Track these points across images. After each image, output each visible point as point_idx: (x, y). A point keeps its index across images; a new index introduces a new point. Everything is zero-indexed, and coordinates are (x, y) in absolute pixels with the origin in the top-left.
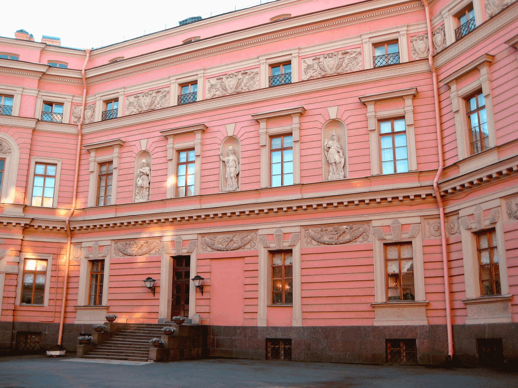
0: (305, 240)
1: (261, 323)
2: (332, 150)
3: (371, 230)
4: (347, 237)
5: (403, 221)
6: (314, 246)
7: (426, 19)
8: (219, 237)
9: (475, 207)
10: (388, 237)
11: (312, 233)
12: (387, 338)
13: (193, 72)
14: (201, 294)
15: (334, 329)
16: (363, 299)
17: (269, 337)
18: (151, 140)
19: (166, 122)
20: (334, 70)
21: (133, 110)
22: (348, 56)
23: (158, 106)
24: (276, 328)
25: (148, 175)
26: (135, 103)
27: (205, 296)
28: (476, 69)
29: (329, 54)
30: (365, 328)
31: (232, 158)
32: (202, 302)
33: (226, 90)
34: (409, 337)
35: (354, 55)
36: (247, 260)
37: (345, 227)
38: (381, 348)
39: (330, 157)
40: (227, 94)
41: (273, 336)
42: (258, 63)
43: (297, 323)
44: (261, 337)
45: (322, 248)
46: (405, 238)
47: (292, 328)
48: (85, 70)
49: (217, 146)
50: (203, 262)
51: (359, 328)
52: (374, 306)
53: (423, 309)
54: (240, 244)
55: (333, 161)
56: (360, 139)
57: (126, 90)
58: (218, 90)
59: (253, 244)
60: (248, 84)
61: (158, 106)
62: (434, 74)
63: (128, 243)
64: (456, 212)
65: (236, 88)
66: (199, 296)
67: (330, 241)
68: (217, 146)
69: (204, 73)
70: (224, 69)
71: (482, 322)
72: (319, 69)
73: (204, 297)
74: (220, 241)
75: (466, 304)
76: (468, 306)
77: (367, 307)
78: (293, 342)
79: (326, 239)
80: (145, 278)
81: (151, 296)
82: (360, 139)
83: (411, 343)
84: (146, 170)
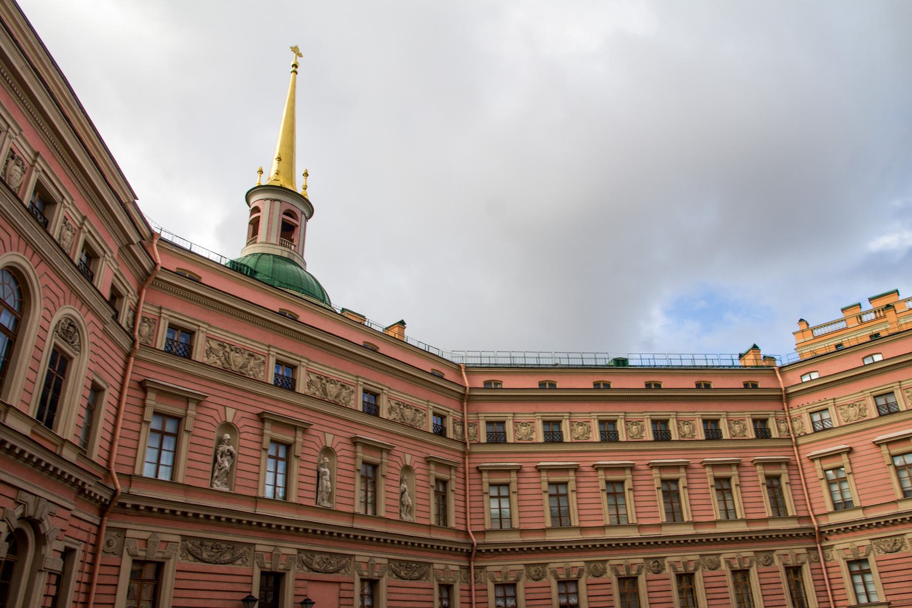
8: (317, 558)
13: (297, 356)
18: (240, 414)
19: (260, 399)
23: (251, 373)
28: (509, 471)
33: (326, 394)
36: (344, 586)
45: (400, 582)
50: (301, 583)
54: (336, 567)
58: (318, 390)
61: (251, 373)
65: (336, 397)
70: (326, 371)
79: (402, 574)
84: (231, 448)
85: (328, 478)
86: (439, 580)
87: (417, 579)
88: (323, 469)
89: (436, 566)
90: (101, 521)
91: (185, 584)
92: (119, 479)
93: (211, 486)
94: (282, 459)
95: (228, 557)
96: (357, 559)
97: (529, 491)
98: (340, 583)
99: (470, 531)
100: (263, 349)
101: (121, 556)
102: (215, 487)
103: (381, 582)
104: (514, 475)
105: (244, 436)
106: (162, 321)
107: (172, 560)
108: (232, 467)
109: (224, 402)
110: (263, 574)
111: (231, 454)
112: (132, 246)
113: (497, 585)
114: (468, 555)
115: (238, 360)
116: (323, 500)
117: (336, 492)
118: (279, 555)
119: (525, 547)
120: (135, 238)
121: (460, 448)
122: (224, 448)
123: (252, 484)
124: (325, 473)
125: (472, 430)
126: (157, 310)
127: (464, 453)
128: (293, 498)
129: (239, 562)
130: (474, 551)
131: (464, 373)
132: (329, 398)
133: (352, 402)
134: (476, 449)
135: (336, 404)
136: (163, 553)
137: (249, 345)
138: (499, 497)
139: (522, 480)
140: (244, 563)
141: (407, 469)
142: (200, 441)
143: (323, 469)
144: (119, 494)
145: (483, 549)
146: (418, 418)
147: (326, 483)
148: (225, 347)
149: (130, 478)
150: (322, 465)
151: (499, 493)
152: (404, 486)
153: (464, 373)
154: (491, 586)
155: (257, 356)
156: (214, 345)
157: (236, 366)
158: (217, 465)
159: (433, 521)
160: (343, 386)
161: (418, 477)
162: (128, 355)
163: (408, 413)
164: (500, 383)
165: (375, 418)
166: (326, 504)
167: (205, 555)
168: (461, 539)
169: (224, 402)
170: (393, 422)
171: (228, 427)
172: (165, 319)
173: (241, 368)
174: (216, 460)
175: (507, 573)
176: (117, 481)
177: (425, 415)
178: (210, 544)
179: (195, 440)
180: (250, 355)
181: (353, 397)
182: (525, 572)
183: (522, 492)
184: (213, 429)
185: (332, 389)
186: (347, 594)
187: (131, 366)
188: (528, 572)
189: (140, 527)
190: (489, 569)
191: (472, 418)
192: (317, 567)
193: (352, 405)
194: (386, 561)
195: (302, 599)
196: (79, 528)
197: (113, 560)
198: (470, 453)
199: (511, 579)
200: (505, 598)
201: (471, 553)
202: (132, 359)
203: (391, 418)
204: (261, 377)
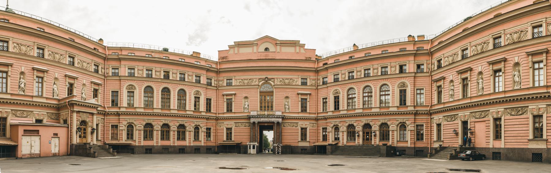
4: (520, 113)
15: (515, 149)
16: (526, 138)
22: (523, 33)
34: (540, 152)
38: (530, 156)
41: (494, 151)
43: (503, 146)
44: (491, 151)
51: (523, 148)
52: (529, 140)
53: (545, 142)
56: (526, 71)
77: (527, 141)
79: (513, 113)
82: (526, 71)
87: (521, 114)
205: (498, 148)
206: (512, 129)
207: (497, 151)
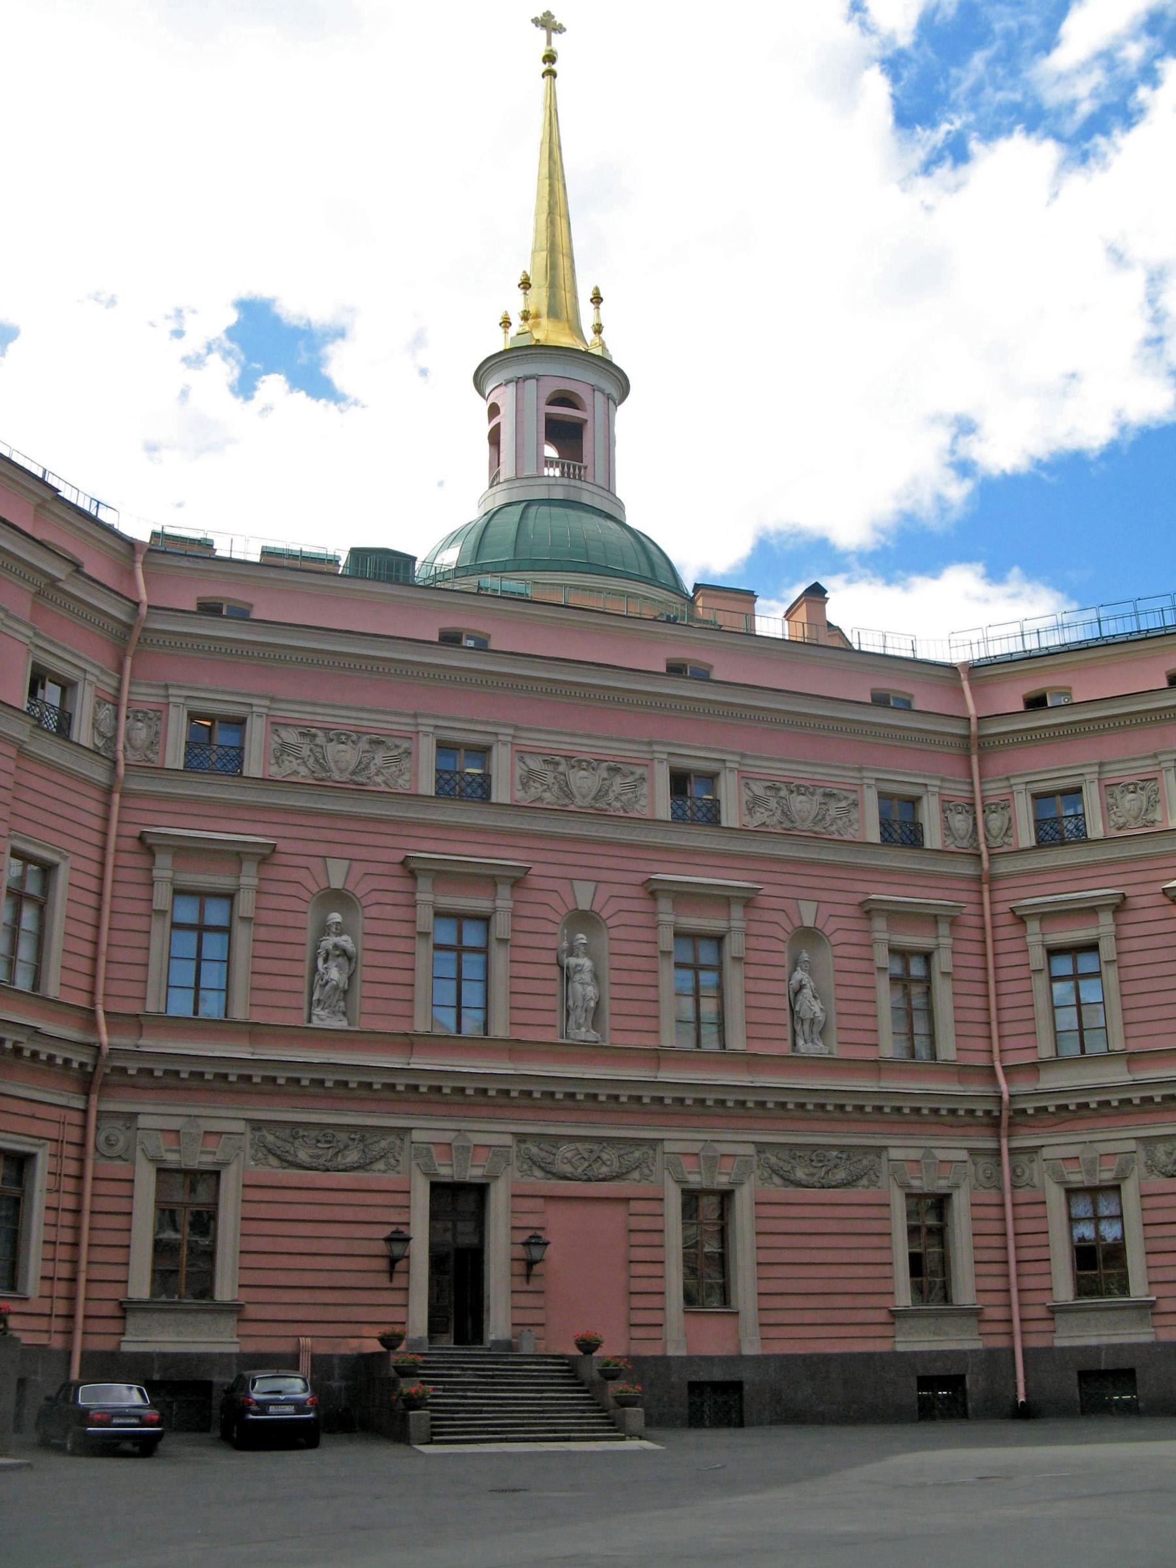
0: (758, 1172)
1: (675, 1350)
2: (807, 992)
3: (885, 1167)
4: (841, 1175)
5: (942, 1155)
6: (777, 1190)
7: (971, 776)
8: (566, 1150)
9: (1082, 1146)
10: (916, 1183)
11: (773, 1160)
12: (921, 1373)
13: (487, 723)
14: (523, 1279)
15: (827, 1359)
17: (694, 1378)
18: (359, 868)
20: (807, 825)
21: (295, 767)
22: (833, 805)
24: (709, 1360)
25: (350, 959)
26: (305, 752)
27: (535, 1284)
28: (1094, 910)
29: (801, 786)
30: (881, 1355)
31: (586, 962)
32: (524, 1300)
35: (843, 804)
36: (635, 1206)
37: (835, 1153)
38: (910, 1394)
39: (805, 1007)
40: (572, 808)
41: (703, 1376)
42: (648, 756)
43: (752, 1348)
46: (941, 1187)
47: (741, 1358)
48: (149, 607)
49: (550, 928)
51: (870, 1356)
52: (893, 1314)
53: (973, 1321)
54: (616, 1167)
55: (809, 1016)
56: (859, 980)
57: (275, 706)
59: (646, 1171)
60: (623, 798)
61: (379, 779)
62: (986, 887)
63: (301, 1133)
64: (1036, 1149)
66: (520, 1284)
67: (812, 1180)
68: (550, 928)
69: (514, 737)
70: (566, 744)
71: (1093, 1341)
72: (779, 812)
73: (530, 1288)
74: (569, 1155)
75: (1053, 1312)
76: (1057, 1316)
77: (883, 1316)
78: (746, 1387)
79: (800, 1174)
80: (387, 1231)
81: (382, 1280)
83: (956, 1382)
84: (345, 941)
85: (587, 977)
86: (903, 1186)
88: (573, 961)
89: (894, 1154)
90: (87, 1102)
91: (264, 1211)
92: (107, 1023)
93: (310, 1021)
94: (473, 950)
95: (353, 1157)
96: (669, 1147)
97: (1148, 957)
98: (628, 1200)
99: (998, 1065)
100: (402, 724)
101: (134, 1163)
102: (316, 1022)
103: (737, 1195)
104: (1106, 918)
105: (374, 911)
106: (173, 712)
107: (233, 1168)
108: (350, 978)
109: (321, 849)
110: (437, 1188)
111: (344, 953)
112: (60, 584)
113: (1071, 1192)
114: (993, 1122)
115: (343, 757)
116: (579, 1027)
117: (607, 1005)
118: (465, 1149)
119: (1136, 1096)
120: (58, 570)
121: (966, 868)
122: (329, 942)
123: (399, 1008)
124: (579, 969)
125: (996, 821)
126: (161, 692)
127: (979, 880)
128: (500, 1029)
129: (380, 1165)
130: (1005, 1115)
131: (966, 685)
132: (579, 801)
133: (643, 802)
134: (1004, 867)
135: (601, 814)
136: (214, 1153)
137: (368, 721)
138: (1076, 977)
139: (1128, 931)
140: (390, 1168)
141: (809, 936)
142: (275, 934)
143: (573, 961)
144: (105, 1051)
145: (1030, 1106)
146: (833, 813)
147: (584, 990)
148: (314, 736)
149: (138, 1022)
150: (571, 952)
151: (1075, 968)
152: (799, 975)
153: (966, 685)
154: (1055, 1197)
155: (390, 742)
156: (290, 736)
157: (341, 771)
158: (317, 978)
159: (889, 1047)
160: (615, 770)
161: (840, 951)
162: (109, 791)
163: (801, 805)
164: (1066, 692)
165: (709, 830)
166: (585, 1034)
167: (303, 1156)
168: (976, 1088)
169: (321, 849)
170: (760, 833)
171: (338, 898)
172: (177, 705)
173: (353, 773)
174: (315, 969)
175: (1093, 1162)
176: (103, 1028)
177: (855, 804)
178: (314, 1133)
179: (263, 933)
180: (372, 742)
181: (645, 789)
182: (1141, 1156)
183: (1128, 959)
184: (302, 907)
185: (583, 782)
186: (645, 1223)
187: (115, 809)
188: (1151, 1156)
189: (173, 1110)
190: (1046, 1153)
191: (995, 789)
192: (567, 1169)
193: (641, 810)
194: (750, 1150)
195: (524, 1236)
196: (33, 1117)
197: (118, 1169)
198: (993, 879)
199: (1106, 1176)
200: (1096, 1219)
201: (998, 1120)
202: (116, 797)
203: (752, 823)
204: (403, 784)
205: (725, 1361)
206: (806, 1257)
207: (718, 1375)
